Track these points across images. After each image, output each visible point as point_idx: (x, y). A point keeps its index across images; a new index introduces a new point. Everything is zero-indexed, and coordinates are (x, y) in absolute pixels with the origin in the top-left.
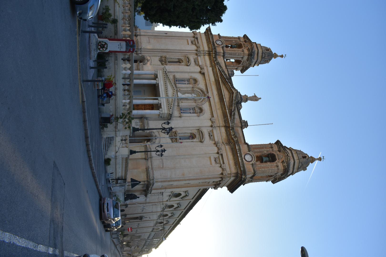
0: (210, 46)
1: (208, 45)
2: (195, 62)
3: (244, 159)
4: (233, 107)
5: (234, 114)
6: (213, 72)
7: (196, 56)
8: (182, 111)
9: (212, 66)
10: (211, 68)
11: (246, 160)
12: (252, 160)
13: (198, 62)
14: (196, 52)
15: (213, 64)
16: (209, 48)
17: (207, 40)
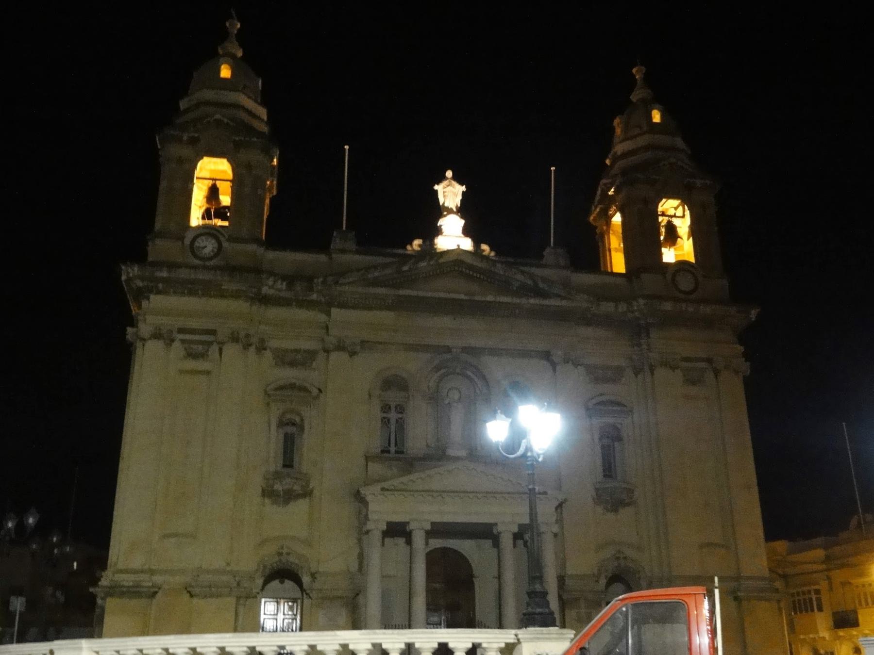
0: (233, 287)
1: (222, 295)
2: (293, 364)
3: (207, 263)
4: (519, 277)
5: (544, 280)
6: (355, 307)
7: (268, 354)
8: (393, 449)
9: (326, 307)
10: (334, 311)
11: (211, 259)
12: (693, 274)
13: (297, 351)
14: (252, 349)
15: (314, 297)
16: (236, 295)
17: (192, 293)
